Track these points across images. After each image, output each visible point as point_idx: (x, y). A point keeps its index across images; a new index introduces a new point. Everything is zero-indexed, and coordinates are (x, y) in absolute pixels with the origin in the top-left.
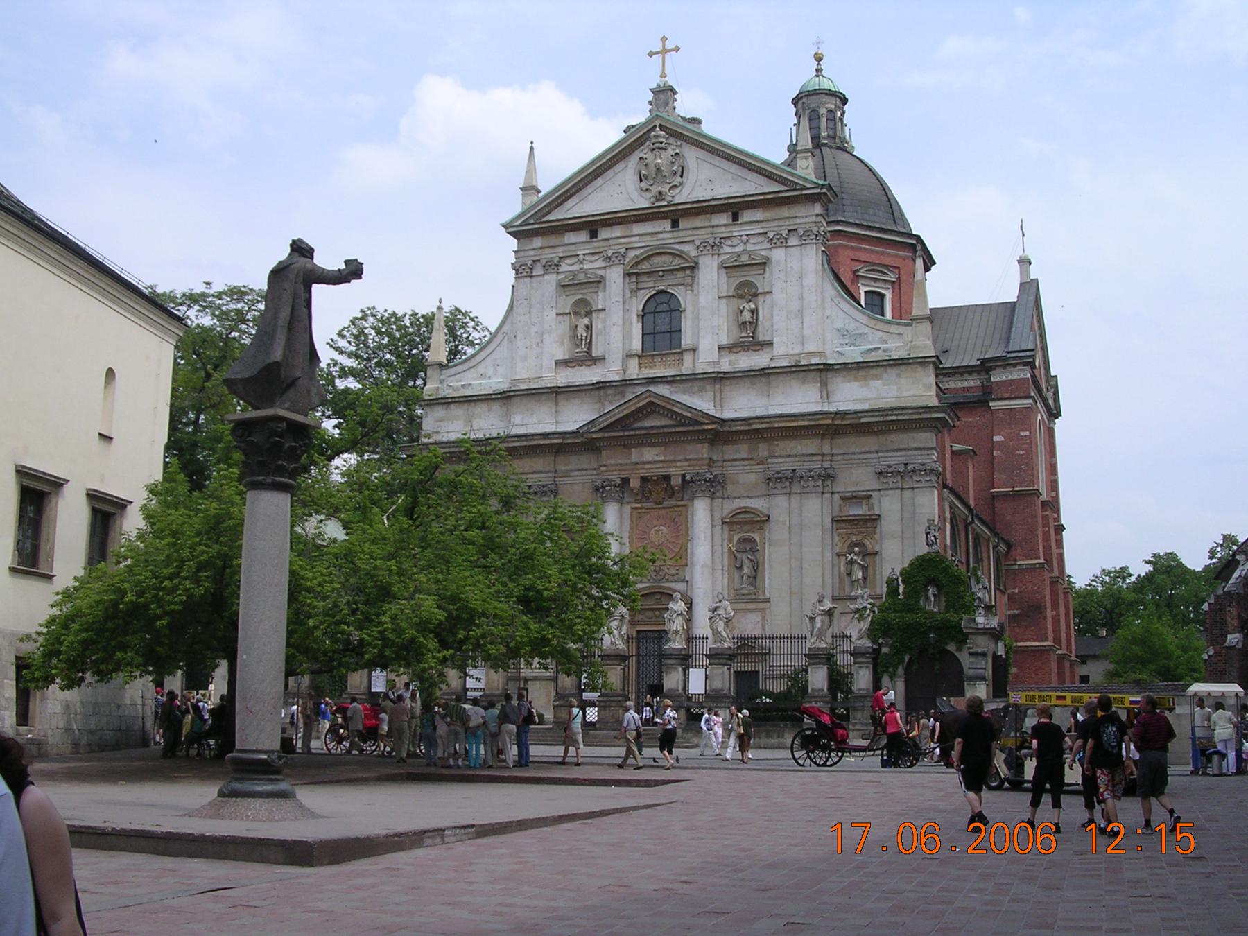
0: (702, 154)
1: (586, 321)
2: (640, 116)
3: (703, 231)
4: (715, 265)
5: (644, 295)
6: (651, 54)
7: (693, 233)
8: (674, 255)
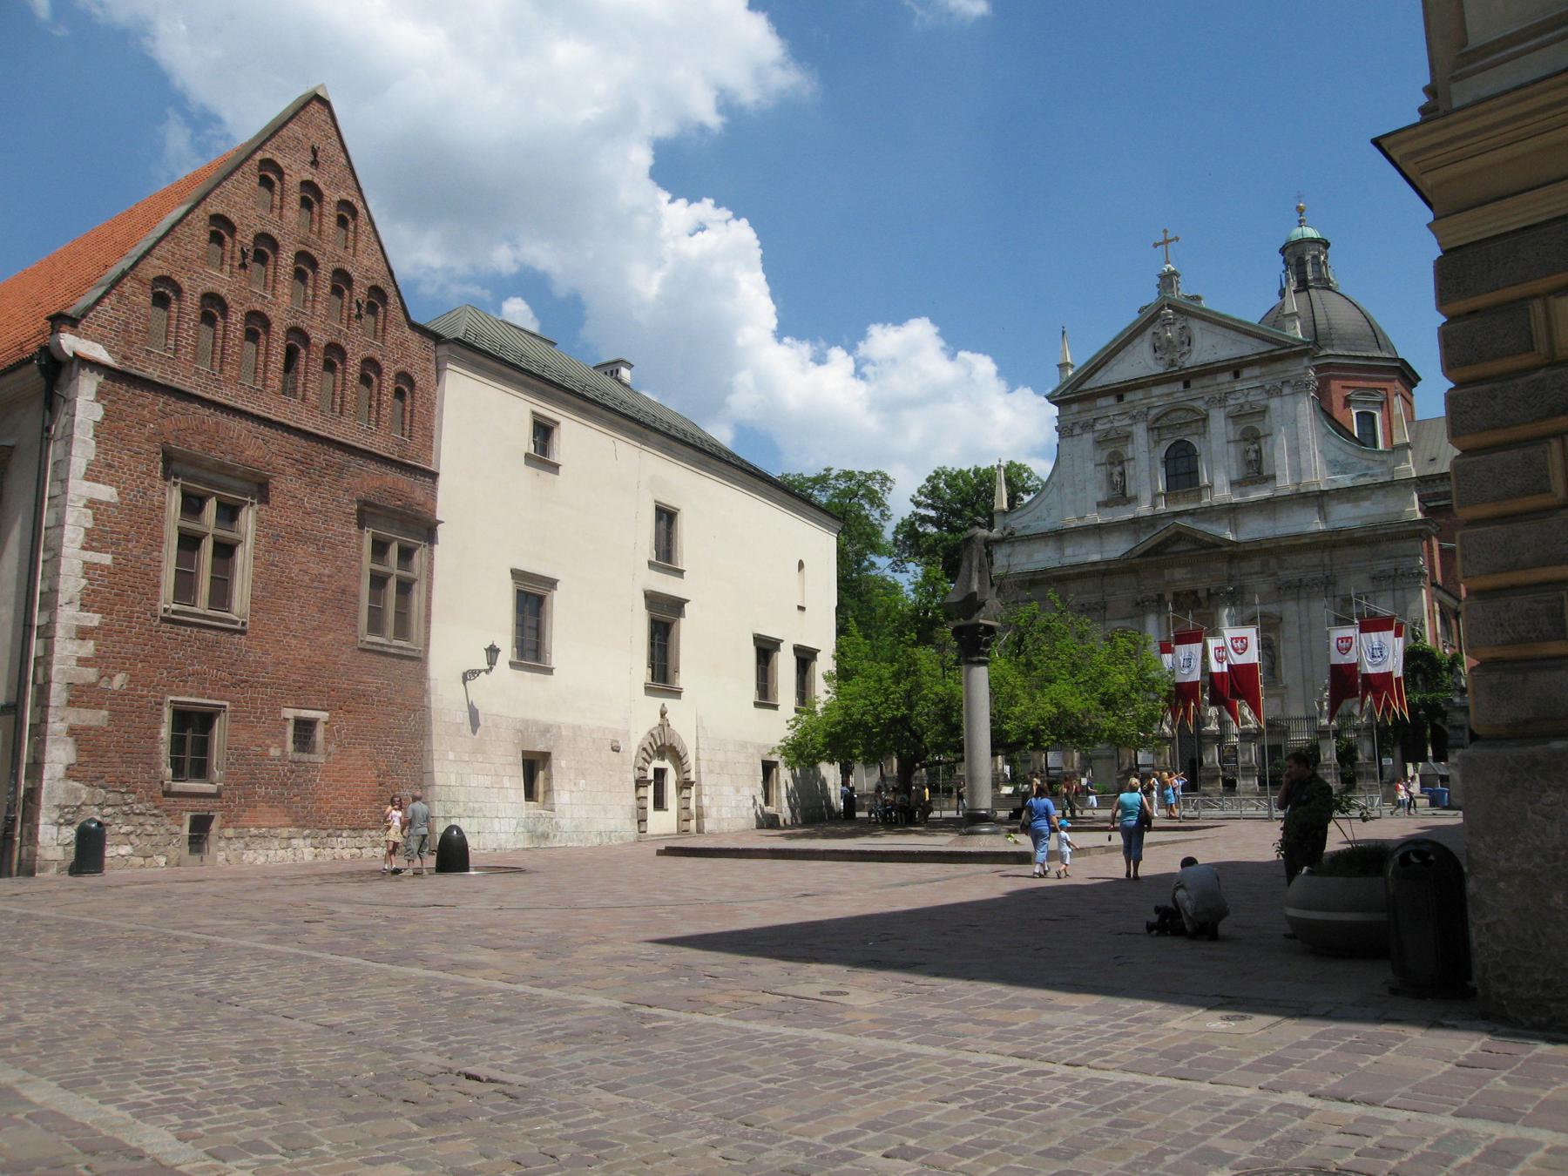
0: (1205, 325)
1: (1119, 469)
2: (1150, 296)
3: (1210, 389)
4: (1222, 415)
5: (1165, 445)
6: (1156, 245)
7: (1200, 392)
8: (1187, 410)
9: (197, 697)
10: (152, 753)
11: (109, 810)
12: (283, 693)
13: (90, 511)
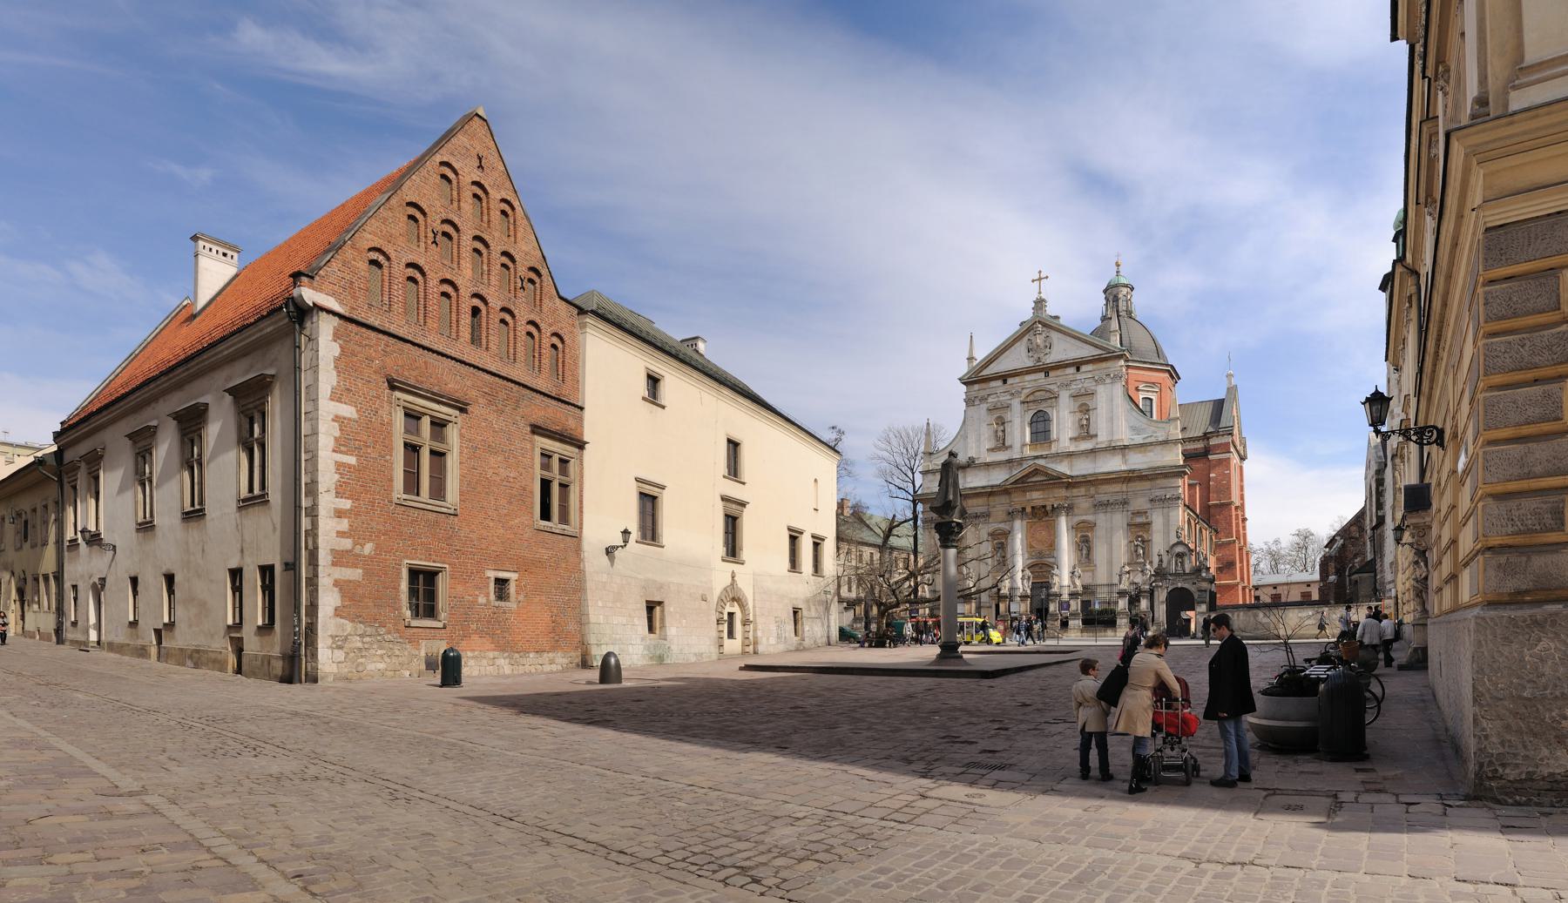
9: (425, 561)
10: (396, 598)
11: (367, 639)
13: (336, 424)
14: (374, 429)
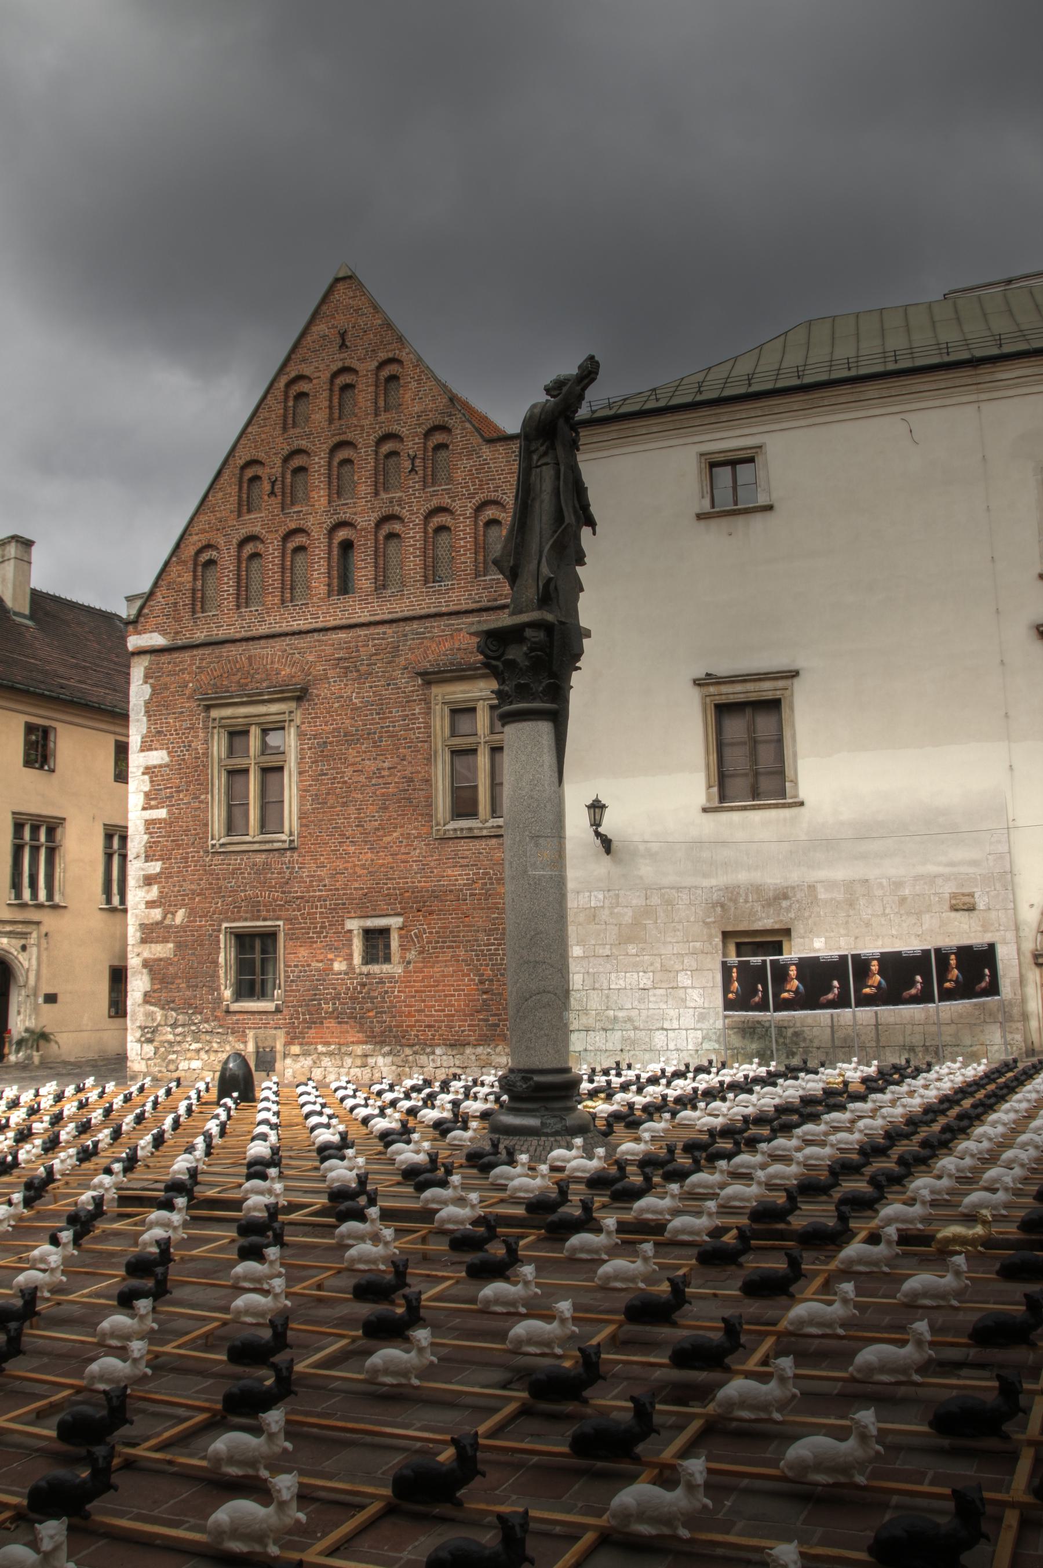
9: (252, 920)
12: (344, 904)
13: (146, 777)
14: (188, 768)
